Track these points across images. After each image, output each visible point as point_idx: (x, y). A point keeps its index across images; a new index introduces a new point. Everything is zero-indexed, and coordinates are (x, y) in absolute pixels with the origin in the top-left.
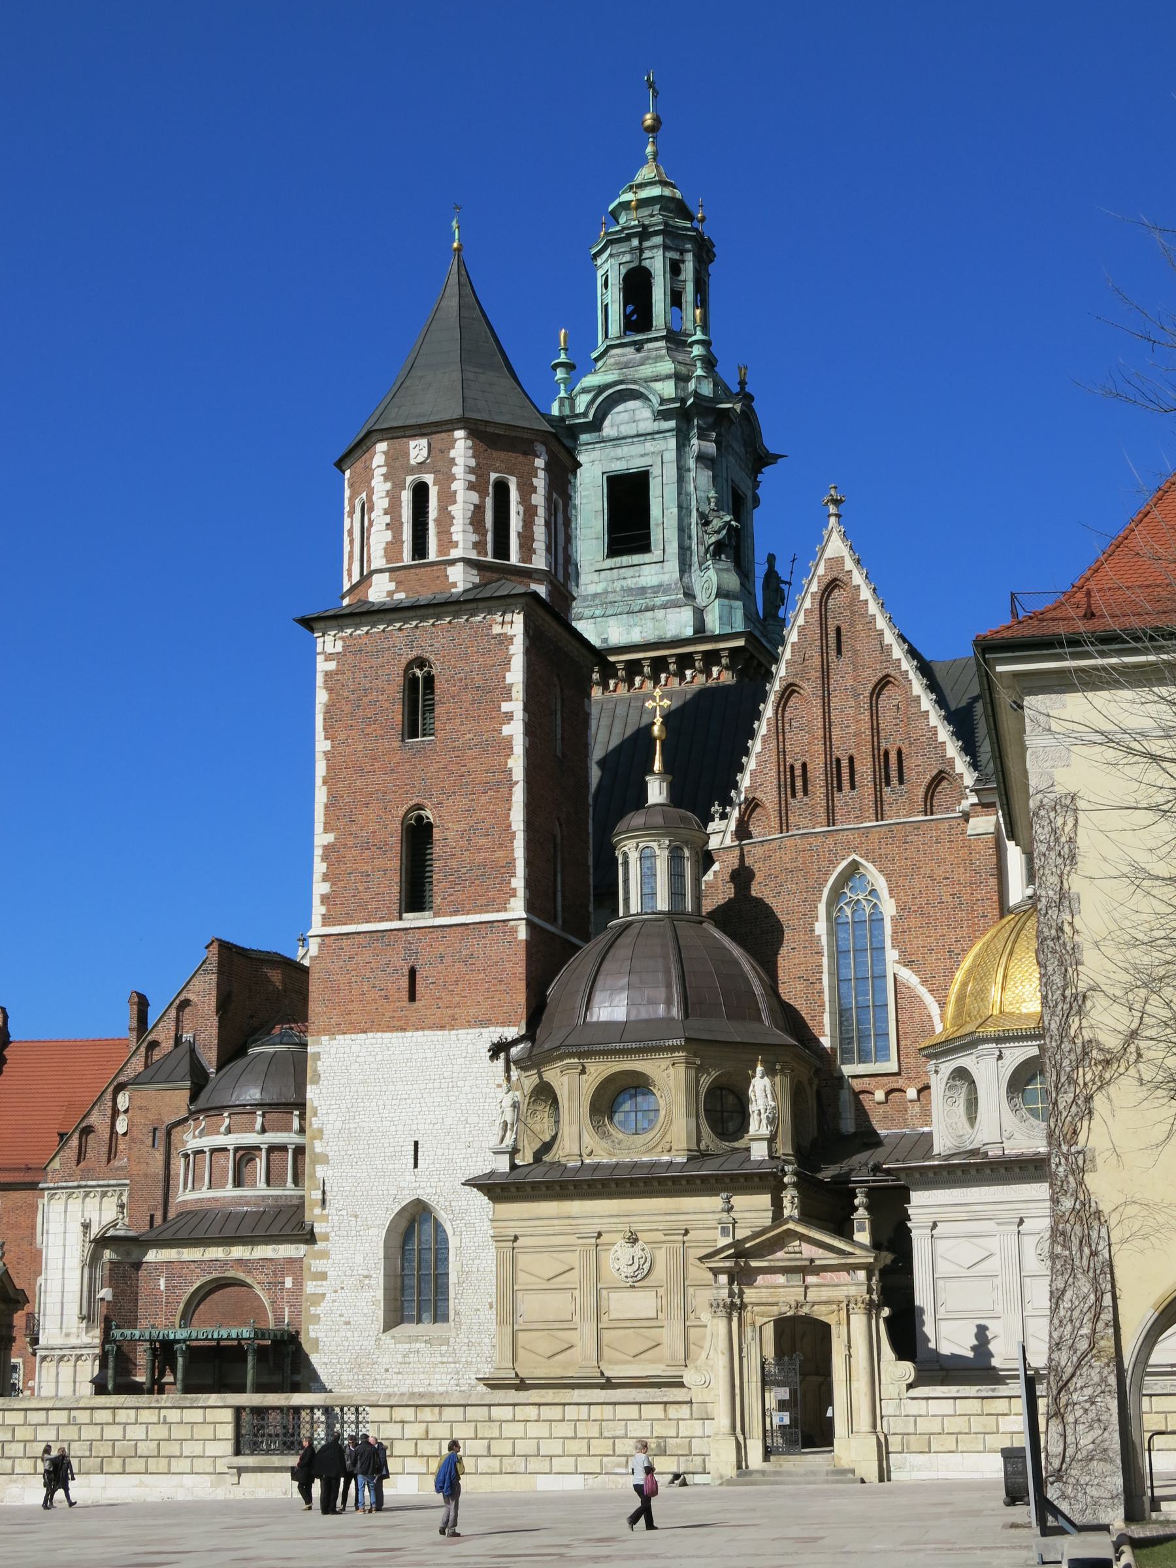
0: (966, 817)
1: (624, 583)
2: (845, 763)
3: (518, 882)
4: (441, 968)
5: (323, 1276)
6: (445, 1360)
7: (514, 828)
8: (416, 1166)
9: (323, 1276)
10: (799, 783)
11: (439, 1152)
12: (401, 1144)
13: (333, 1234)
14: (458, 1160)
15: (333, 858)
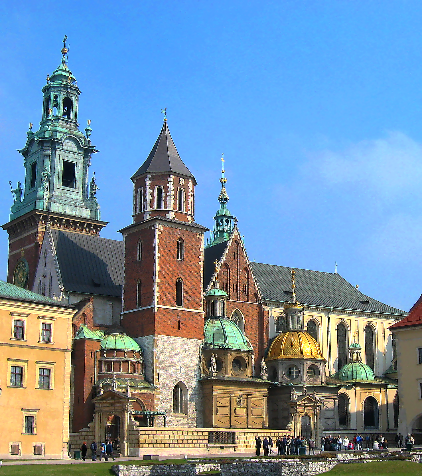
0: (260, 306)
1: (66, 194)
2: (235, 285)
3: (202, 303)
4: (186, 322)
5: (159, 399)
6: (187, 423)
7: (201, 289)
8: (180, 373)
9: (159, 399)
10: (225, 288)
11: (185, 369)
12: (177, 366)
13: (161, 388)
14: (189, 372)
15: (160, 286)
